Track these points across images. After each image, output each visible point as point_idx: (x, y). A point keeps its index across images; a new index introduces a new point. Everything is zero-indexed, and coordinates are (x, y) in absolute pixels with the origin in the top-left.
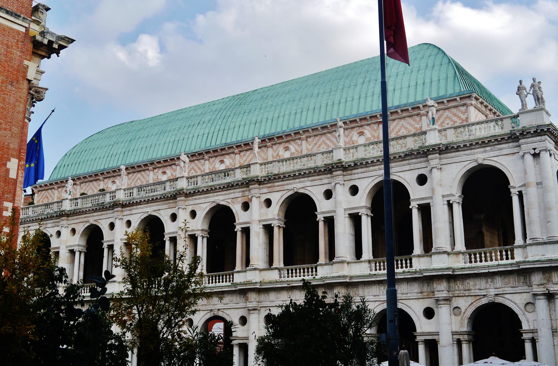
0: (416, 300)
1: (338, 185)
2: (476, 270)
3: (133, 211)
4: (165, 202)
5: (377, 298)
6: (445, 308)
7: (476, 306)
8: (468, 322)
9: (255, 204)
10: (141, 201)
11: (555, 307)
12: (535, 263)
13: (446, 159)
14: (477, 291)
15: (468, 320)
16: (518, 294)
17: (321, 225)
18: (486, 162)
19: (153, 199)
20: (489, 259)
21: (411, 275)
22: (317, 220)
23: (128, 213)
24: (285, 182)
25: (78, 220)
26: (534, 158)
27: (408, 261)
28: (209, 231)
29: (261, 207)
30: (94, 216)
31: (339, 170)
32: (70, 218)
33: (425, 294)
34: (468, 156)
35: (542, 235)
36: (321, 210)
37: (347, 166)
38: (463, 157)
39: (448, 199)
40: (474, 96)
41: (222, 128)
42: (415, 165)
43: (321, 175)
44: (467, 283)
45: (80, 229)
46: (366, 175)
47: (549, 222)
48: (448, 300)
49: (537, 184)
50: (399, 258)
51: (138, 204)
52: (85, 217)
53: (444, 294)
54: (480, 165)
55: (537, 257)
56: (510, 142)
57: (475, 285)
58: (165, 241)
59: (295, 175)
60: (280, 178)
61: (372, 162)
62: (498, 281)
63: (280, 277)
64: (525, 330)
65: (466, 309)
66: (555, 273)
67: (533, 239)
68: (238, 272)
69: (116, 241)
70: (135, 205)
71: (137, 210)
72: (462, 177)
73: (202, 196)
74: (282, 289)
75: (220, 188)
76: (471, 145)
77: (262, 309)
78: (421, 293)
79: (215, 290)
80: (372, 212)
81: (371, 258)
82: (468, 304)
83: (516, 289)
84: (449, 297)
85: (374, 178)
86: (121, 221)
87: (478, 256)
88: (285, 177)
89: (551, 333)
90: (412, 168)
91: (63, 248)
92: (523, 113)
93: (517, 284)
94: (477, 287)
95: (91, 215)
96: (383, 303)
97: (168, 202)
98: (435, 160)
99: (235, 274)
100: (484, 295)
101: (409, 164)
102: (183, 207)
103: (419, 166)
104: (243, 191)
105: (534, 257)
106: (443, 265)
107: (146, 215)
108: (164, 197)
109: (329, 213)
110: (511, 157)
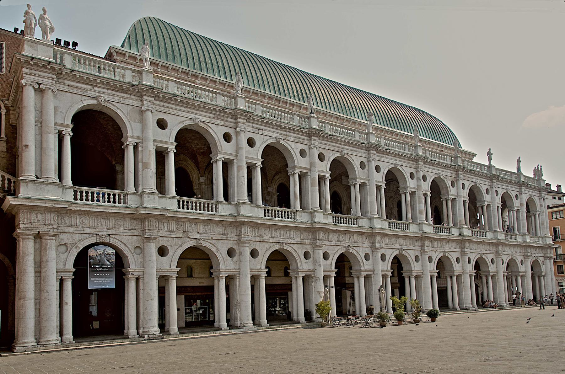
3: (382, 158)
4: (407, 161)
23: (378, 158)
25: (328, 146)
45: (331, 156)
60: (472, 172)
71: (386, 159)
97: (409, 162)
104: (452, 173)
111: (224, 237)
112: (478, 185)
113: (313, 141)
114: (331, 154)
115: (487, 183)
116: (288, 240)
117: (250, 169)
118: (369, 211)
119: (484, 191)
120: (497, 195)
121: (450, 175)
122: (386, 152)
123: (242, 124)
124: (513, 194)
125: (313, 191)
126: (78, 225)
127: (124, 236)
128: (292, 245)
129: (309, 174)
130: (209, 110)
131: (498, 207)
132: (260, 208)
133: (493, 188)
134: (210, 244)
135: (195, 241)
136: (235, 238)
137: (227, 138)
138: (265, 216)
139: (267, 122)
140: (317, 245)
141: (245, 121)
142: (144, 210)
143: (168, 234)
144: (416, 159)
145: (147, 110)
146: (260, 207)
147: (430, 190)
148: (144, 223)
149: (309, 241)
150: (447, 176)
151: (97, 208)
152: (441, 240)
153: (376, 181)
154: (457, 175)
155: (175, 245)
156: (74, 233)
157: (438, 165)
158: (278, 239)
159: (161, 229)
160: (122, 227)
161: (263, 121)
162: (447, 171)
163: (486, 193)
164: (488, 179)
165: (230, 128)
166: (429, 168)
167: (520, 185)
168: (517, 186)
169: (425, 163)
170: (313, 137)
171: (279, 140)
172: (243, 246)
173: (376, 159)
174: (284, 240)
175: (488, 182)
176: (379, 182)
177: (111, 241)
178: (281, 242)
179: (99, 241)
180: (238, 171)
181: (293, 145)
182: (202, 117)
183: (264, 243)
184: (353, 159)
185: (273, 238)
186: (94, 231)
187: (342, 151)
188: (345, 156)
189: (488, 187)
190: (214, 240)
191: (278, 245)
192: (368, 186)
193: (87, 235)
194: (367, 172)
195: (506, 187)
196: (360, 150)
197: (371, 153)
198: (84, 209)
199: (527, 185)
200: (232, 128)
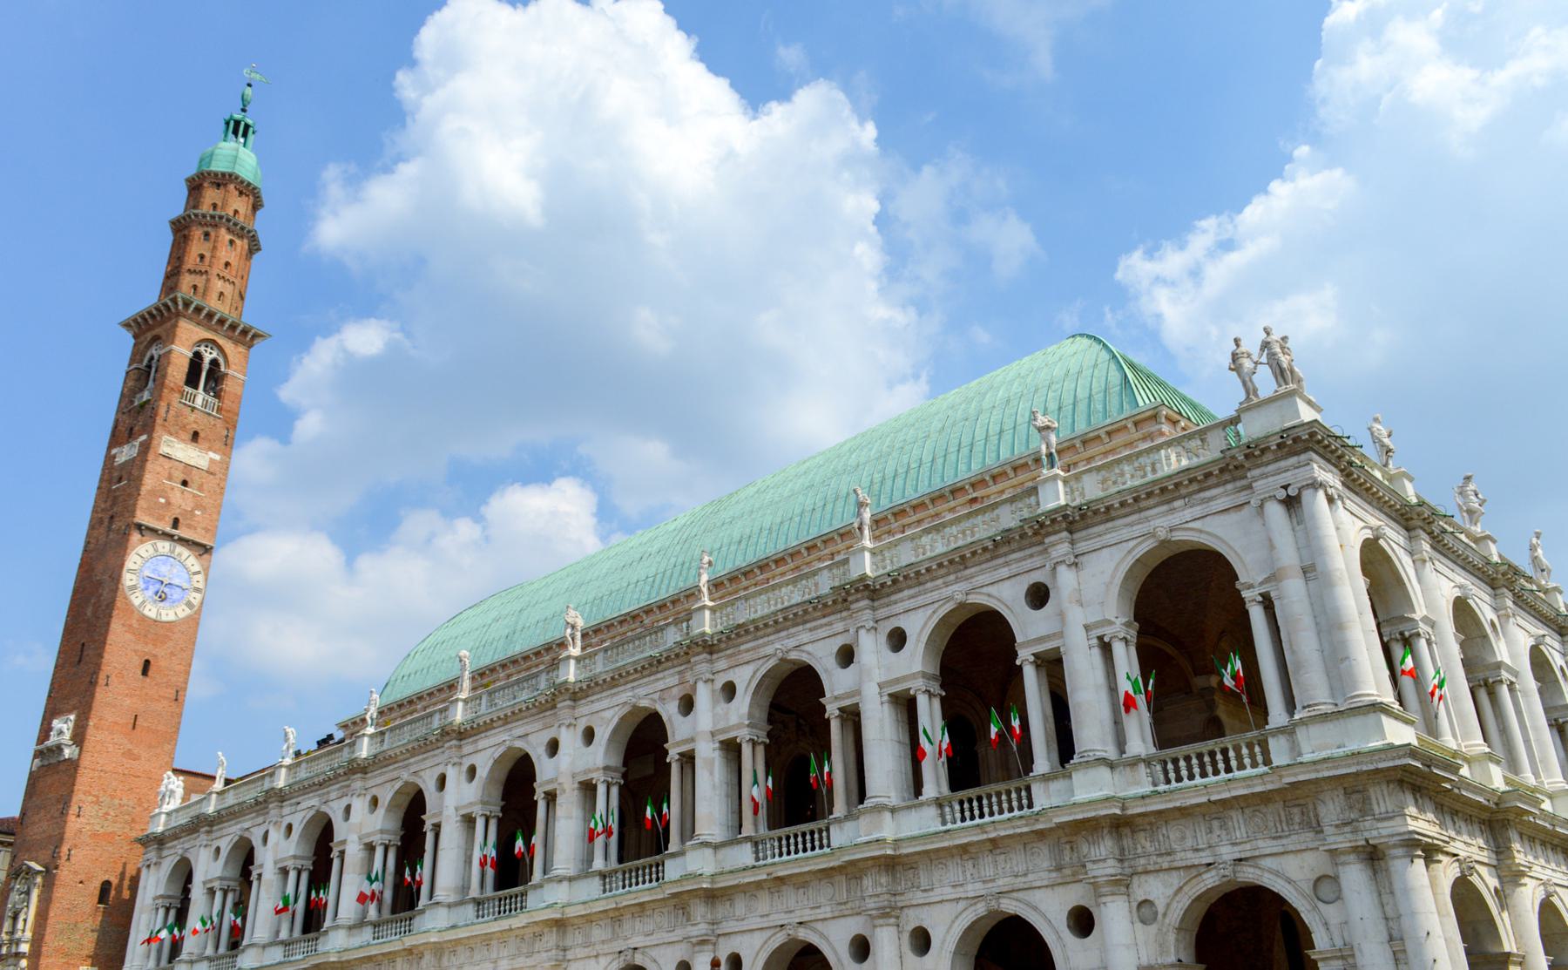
0: (1049, 889)
1: (862, 632)
2: (1178, 799)
5: (960, 893)
6: (1115, 904)
7: (1190, 893)
8: (1177, 940)
9: (704, 697)
10: (492, 720)
11: (1391, 883)
12: (1318, 767)
13: (1087, 540)
14: (1190, 854)
15: (1178, 934)
16: (1291, 856)
17: (835, 726)
18: (1179, 536)
19: (513, 713)
20: (1209, 769)
21: (1026, 825)
22: (826, 716)
24: (761, 641)
26: (1288, 510)
27: (1023, 793)
28: (625, 769)
29: (715, 703)
31: (863, 599)
32: (369, 775)
33: (1068, 872)
34: (1134, 528)
35: (1333, 696)
36: (832, 691)
37: (878, 587)
38: (1125, 531)
39: (1099, 632)
40: (1164, 413)
41: (680, 560)
42: (1020, 564)
43: (829, 615)
44: (1163, 835)
45: (386, 796)
46: (920, 601)
47: (1342, 660)
48: (1122, 884)
49: (1305, 571)
50: (1002, 787)
51: (489, 726)
52: (395, 769)
53: (1110, 868)
54: (1164, 543)
55: (1324, 753)
56: (1226, 482)
57: (1183, 838)
58: (536, 802)
59: (776, 622)
60: (747, 632)
61: (928, 570)
62: (1236, 826)
63: (757, 859)
64: (1320, 952)
65: (1168, 905)
66: (1377, 788)
67: (1309, 706)
68: (673, 855)
69: (445, 813)
70: (483, 732)
72: (1126, 578)
73: (604, 694)
74: (759, 885)
75: (636, 670)
76: (1136, 499)
77: (721, 940)
78: (1059, 869)
79: (625, 904)
80: (942, 686)
81: (945, 790)
82: (1170, 892)
83: (1284, 841)
84: (1121, 874)
85: (936, 605)
86: (456, 768)
87: (1182, 764)
88: (757, 628)
89: (1389, 955)
90: (1015, 571)
91: (353, 842)
92: (1248, 409)
93: (1286, 828)
94: (1189, 843)
95: (406, 762)
96: (975, 904)
97: (541, 715)
98: (1060, 547)
99: (667, 863)
100: (1210, 864)
101: (1007, 564)
102: (567, 722)
103: (1028, 564)
105: (1316, 754)
106: (1101, 793)
107: (501, 750)
108: (534, 705)
109: (848, 698)
110: (1233, 517)
121: (674, 680)
157: (616, 680)
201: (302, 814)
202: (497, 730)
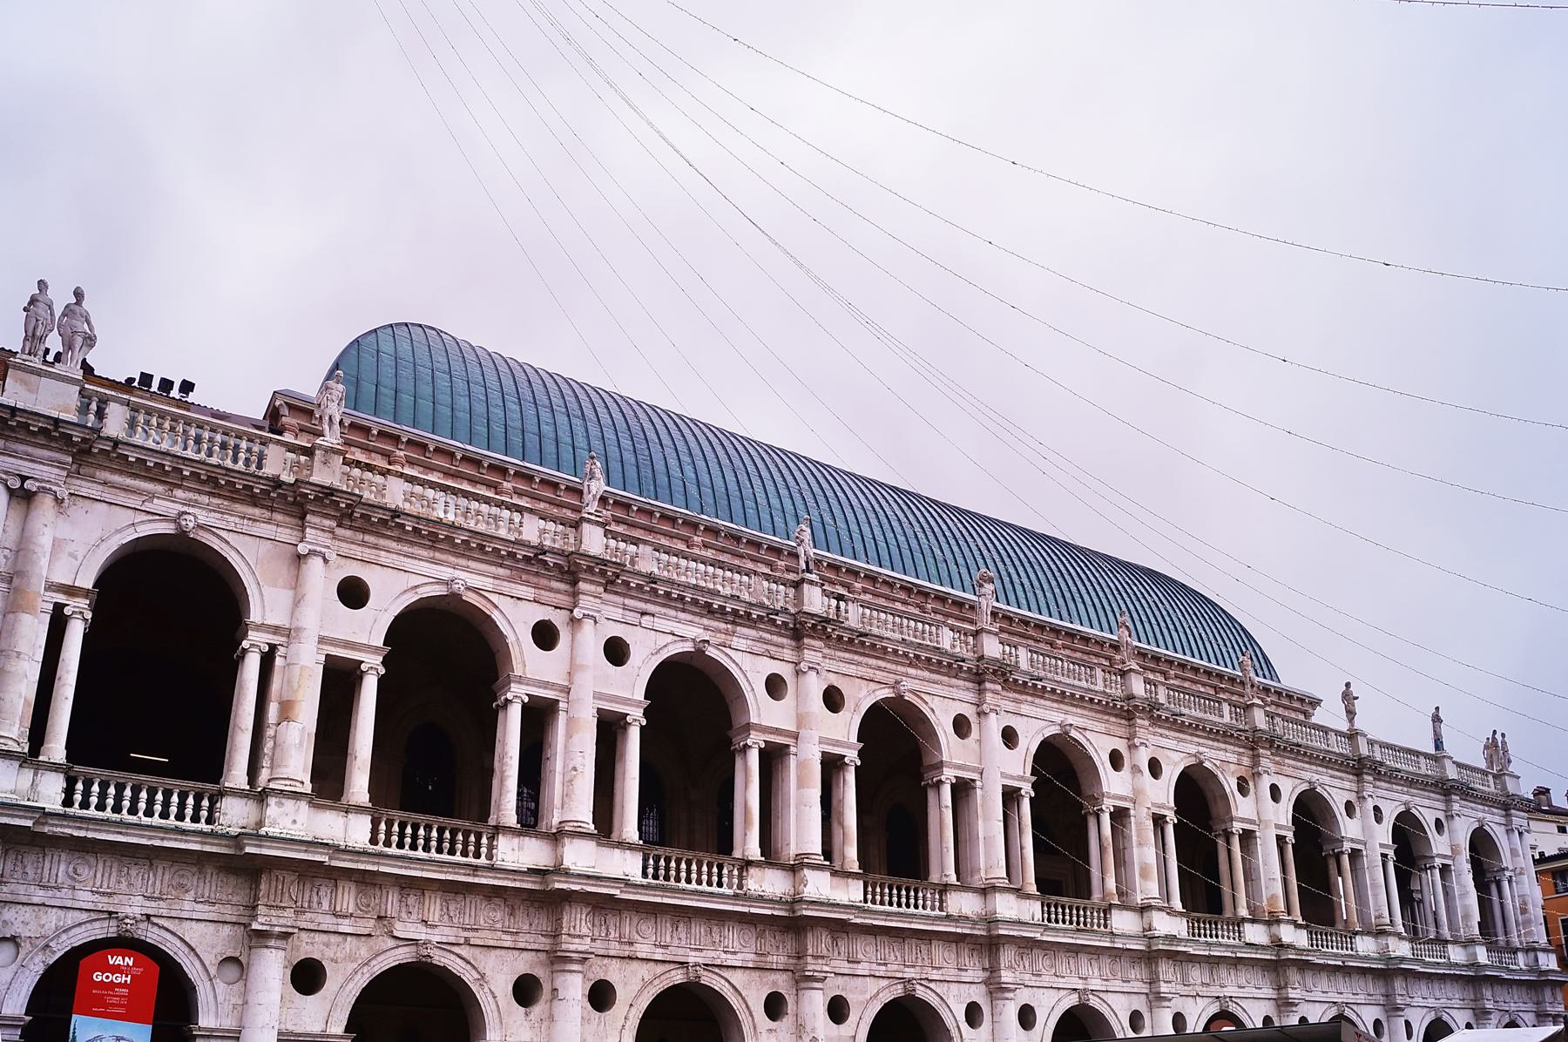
3: (1022, 706)
4: (1100, 716)
19: (1082, 698)
23: (1011, 706)
30: (907, 675)
33: (1466, 1002)
45: (861, 697)
52: (879, 668)
71: (1034, 709)
78: (1463, 1000)
90: (1431, 805)
97: (1106, 717)
104: (1240, 754)
111: (507, 941)
112: (1319, 789)
113: (806, 651)
114: (864, 692)
115: (1347, 785)
116: (713, 954)
117: (610, 729)
118: (982, 866)
119: (1339, 809)
120: (1379, 819)
122: (1031, 689)
123: (591, 599)
124: (1428, 817)
125: (801, 803)
126: (59, 881)
127: (194, 922)
128: (726, 974)
129: (792, 749)
130: (497, 558)
131: (1384, 856)
132: (628, 851)
133: (1364, 798)
134: (459, 961)
135: (413, 948)
136: (543, 943)
137: (545, 636)
138: (645, 875)
139: (668, 594)
140: (807, 973)
141: (601, 589)
142: (256, 846)
143: (328, 922)
144: (1126, 712)
145: (312, 553)
146: (629, 849)
147: (1172, 804)
148: (258, 884)
149: (782, 959)
150: (1225, 763)
151: (120, 833)
152: (1213, 962)
153: (1003, 775)
154: (1255, 759)
155: (351, 958)
156: (44, 905)
158: (681, 952)
159: (309, 907)
160: (192, 892)
161: (654, 591)
162: (1223, 746)
163: (1344, 813)
164: (1347, 772)
165: (556, 607)
166: (1167, 737)
167: (1445, 789)
168: (1438, 793)
169: (1156, 721)
170: (806, 641)
171: (701, 645)
172: (564, 971)
173: (1003, 709)
174: (702, 954)
175: (1349, 783)
176: (1012, 778)
177: (152, 935)
178: (691, 960)
179: (115, 935)
180: (569, 736)
181: (746, 661)
182: (474, 576)
183: (635, 964)
184: (931, 706)
185: (666, 947)
186: (103, 903)
187: (897, 682)
188: (908, 697)
189: (1352, 797)
190: (473, 949)
191: (680, 971)
192: (979, 791)
193: (84, 916)
194: (976, 746)
195: (1406, 798)
196: (954, 681)
197: (985, 689)
198: (82, 834)
199: (1466, 792)
200: (560, 608)
201: (664, 639)
202: (1048, 703)
